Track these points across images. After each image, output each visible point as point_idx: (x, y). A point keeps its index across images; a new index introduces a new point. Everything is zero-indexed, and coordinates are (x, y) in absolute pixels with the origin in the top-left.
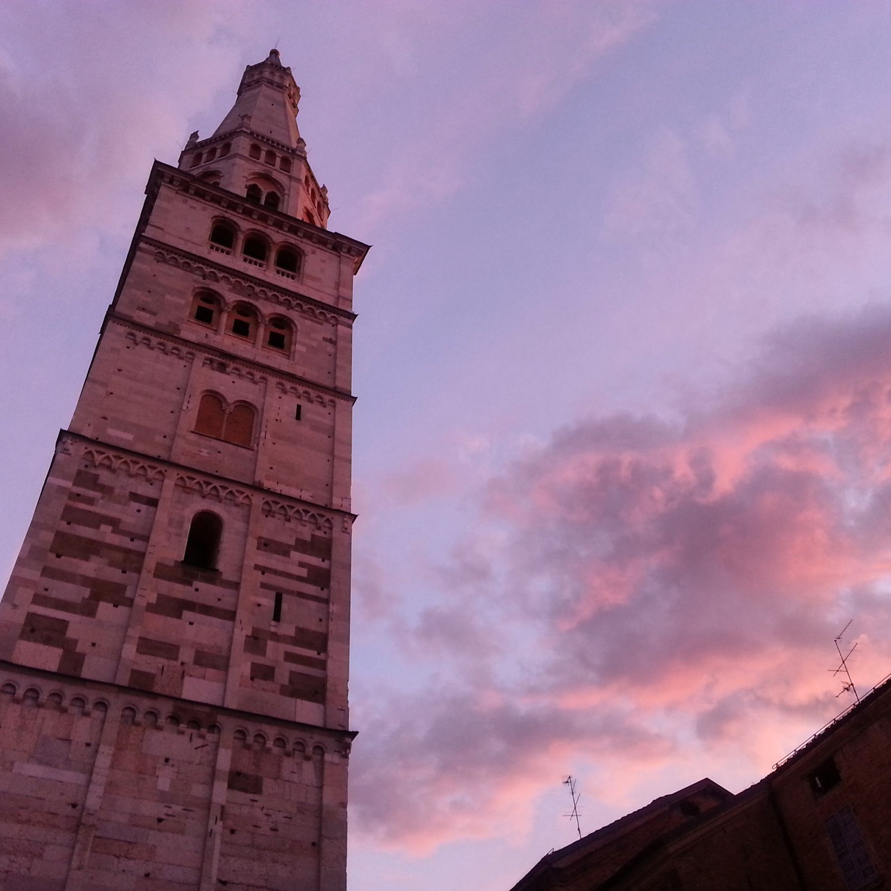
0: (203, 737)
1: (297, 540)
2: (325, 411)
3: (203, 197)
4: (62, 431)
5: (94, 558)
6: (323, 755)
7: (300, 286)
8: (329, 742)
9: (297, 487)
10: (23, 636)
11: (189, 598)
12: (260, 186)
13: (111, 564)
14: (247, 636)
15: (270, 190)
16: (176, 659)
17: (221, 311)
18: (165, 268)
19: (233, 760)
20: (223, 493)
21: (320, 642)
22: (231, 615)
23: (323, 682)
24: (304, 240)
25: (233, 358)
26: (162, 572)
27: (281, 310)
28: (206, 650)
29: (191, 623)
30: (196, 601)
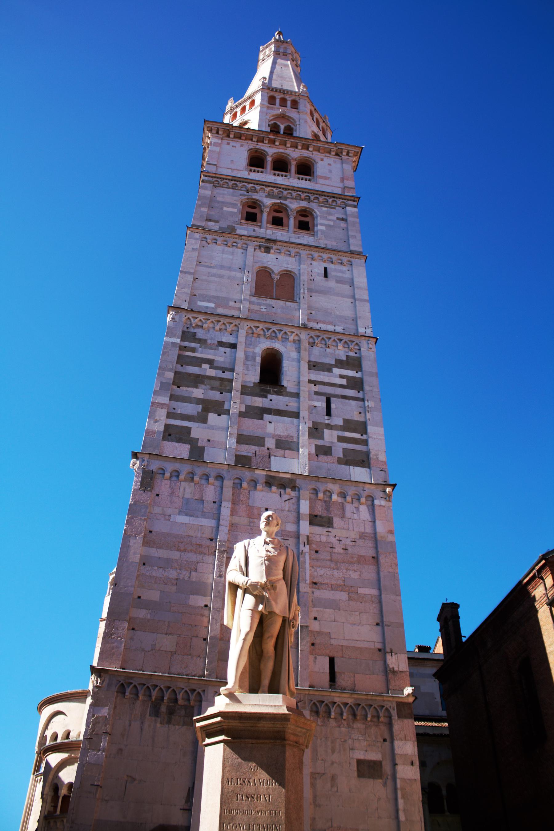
1: (336, 360)
2: (344, 268)
6: (373, 501)
7: (315, 185)
9: (331, 323)
10: (164, 439)
11: (266, 406)
13: (212, 389)
16: (264, 446)
17: (262, 212)
18: (220, 190)
19: (311, 507)
20: (279, 335)
22: (296, 415)
23: (367, 454)
24: (314, 153)
25: (275, 241)
26: (245, 390)
27: (304, 204)
28: (283, 439)
29: (270, 422)
30: (271, 407)
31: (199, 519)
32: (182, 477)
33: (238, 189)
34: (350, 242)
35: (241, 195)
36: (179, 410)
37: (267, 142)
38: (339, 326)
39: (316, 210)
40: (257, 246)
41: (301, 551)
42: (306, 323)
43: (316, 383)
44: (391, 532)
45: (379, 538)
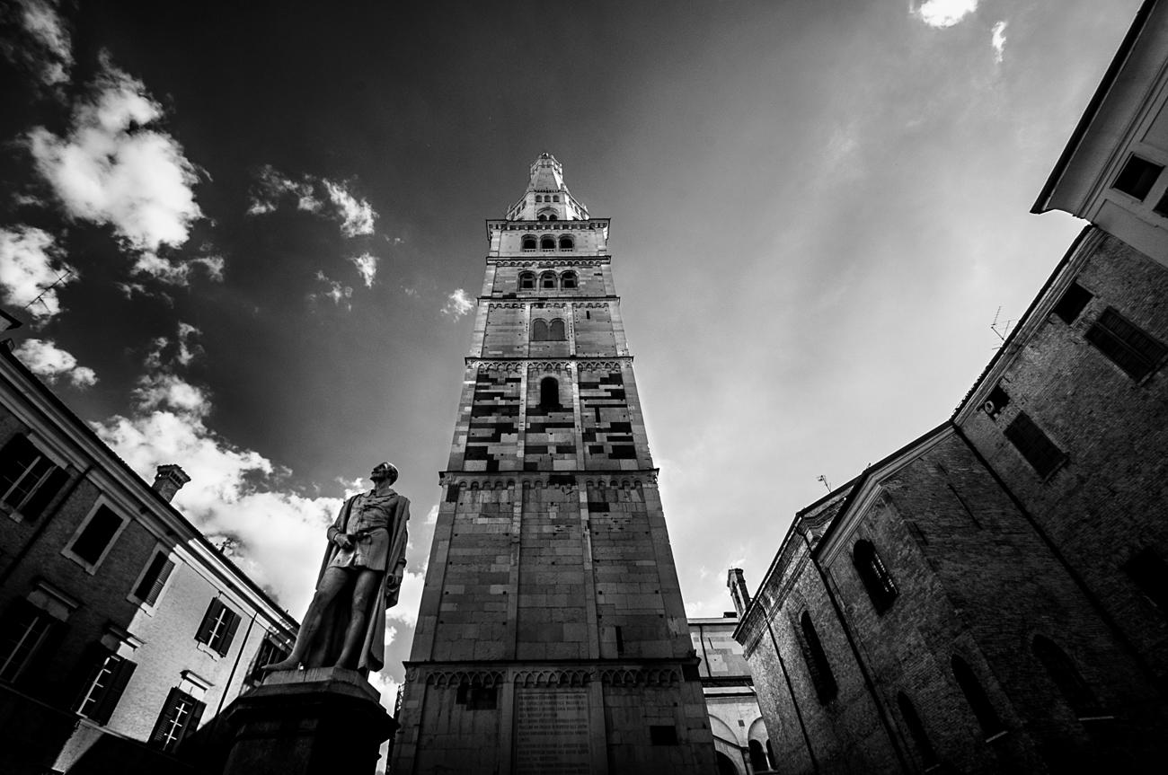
8: (644, 477)
10: (466, 458)
13: (503, 415)
14: (583, 434)
16: (547, 453)
17: (536, 279)
19: (589, 497)
21: (626, 427)
23: (633, 448)
25: (546, 299)
27: (568, 268)
32: (481, 486)
44: (661, 509)
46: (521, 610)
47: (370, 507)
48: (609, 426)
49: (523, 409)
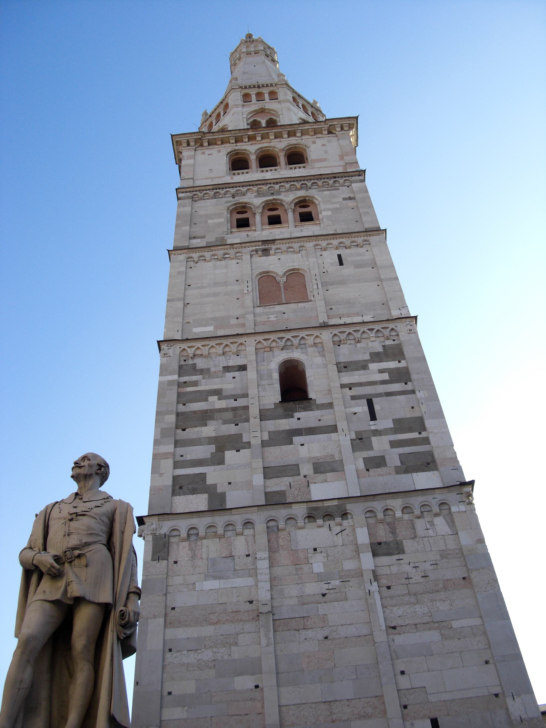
0: (341, 525)
1: (371, 354)
2: (362, 250)
3: (216, 144)
4: (159, 342)
5: (209, 422)
6: (450, 509)
8: (451, 497)
9: (357, 314)
10: (174, 494)
12: (258, 119)
13: (225, 422)
15: (268, 118)
16: (299, 475)
20: (296, 341)
21: (419, 424)
23: (431, 454)
24: (303, 138)
25: (273, 241)
27: (302, 193)
28: (321, 460)
29: (302, 445)
31: (231, 580)
32: (202, 533)
33: (222, 197)
34: (363, 220)
35: (226, 202)
36: (189, 456)
37: (247, 140)
38: (367, 315)
39: (316, 197)
40: (253, 251)
41: (367, 591)
42: (326, 320)
43: (350, 386)
44: (481, 541)
45: (465, 553)
46: (284, 709)
47: (77, 514)
48: (391, 425)
49: (254, 411)
